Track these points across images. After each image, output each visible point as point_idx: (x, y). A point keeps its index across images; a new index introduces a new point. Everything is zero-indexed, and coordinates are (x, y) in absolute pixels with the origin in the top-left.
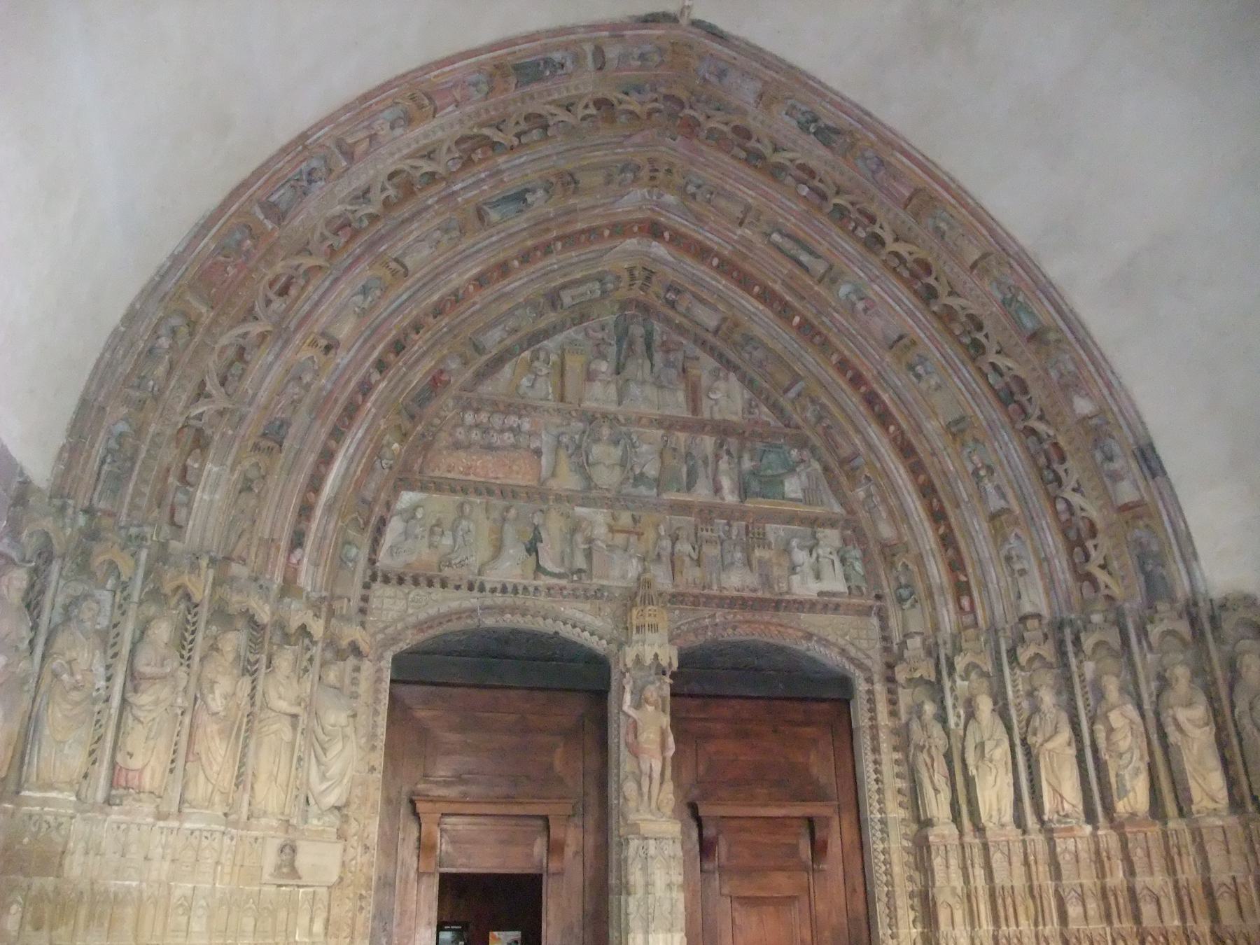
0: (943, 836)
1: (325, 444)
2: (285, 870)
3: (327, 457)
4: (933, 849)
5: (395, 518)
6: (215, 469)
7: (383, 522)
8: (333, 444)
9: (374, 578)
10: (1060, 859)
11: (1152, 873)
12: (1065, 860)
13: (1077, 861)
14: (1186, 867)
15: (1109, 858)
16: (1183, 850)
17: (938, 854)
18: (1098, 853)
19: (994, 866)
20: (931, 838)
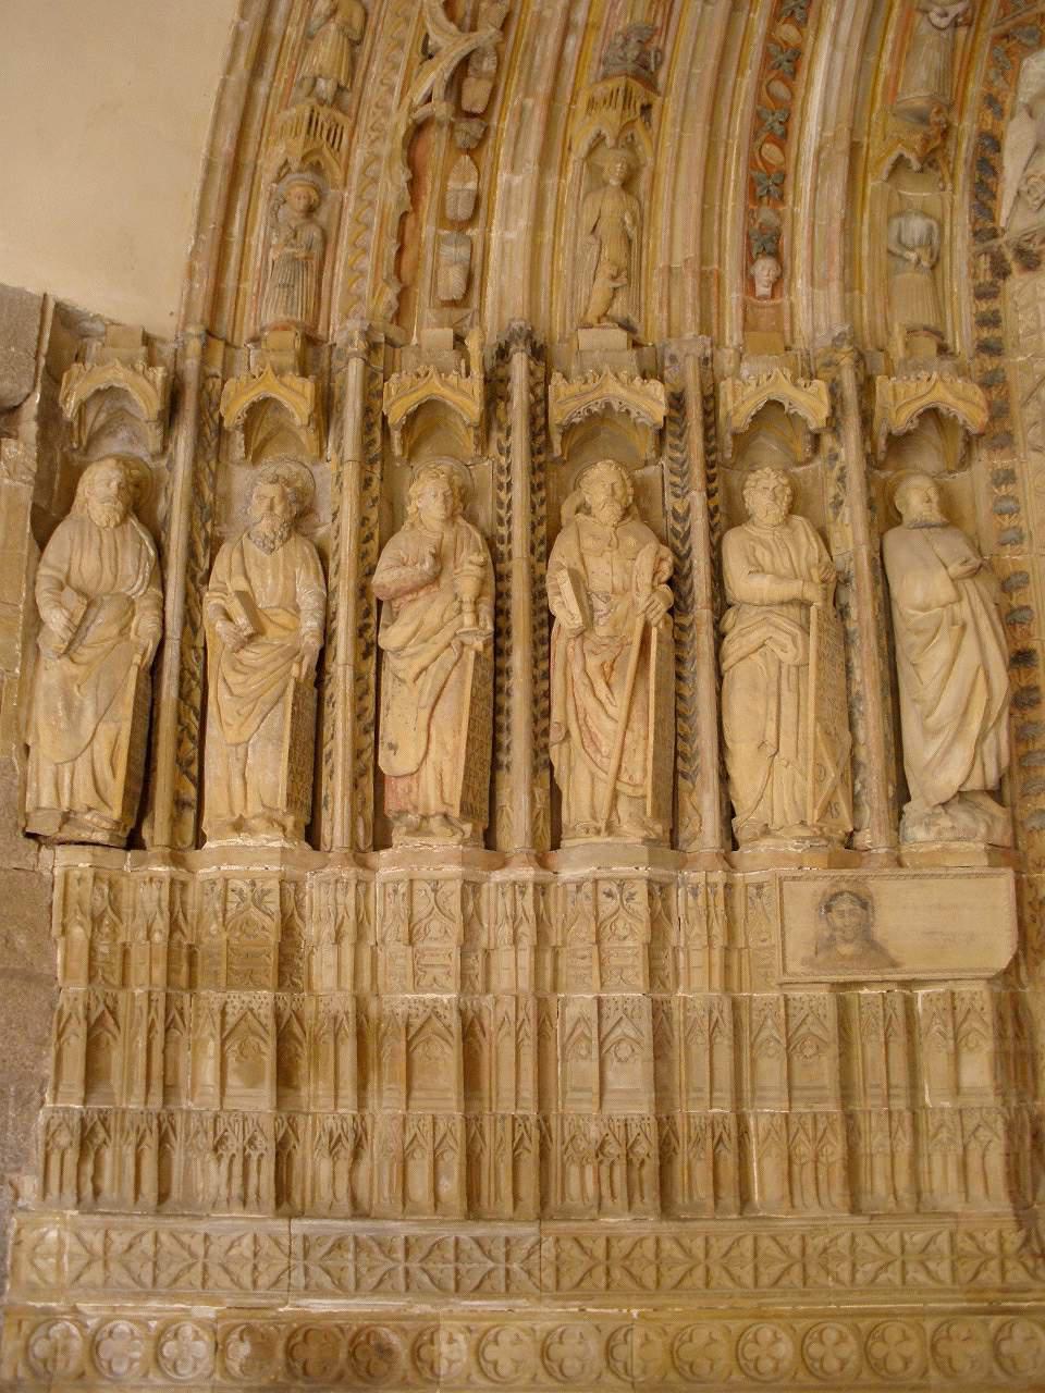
1: (769, 37)
2: (846, 949)
3: (786, 64)
5: (1016, 120)
6: (517, 180)
7: (990, 147)
8: (788, 32)
9: (1000, 271)
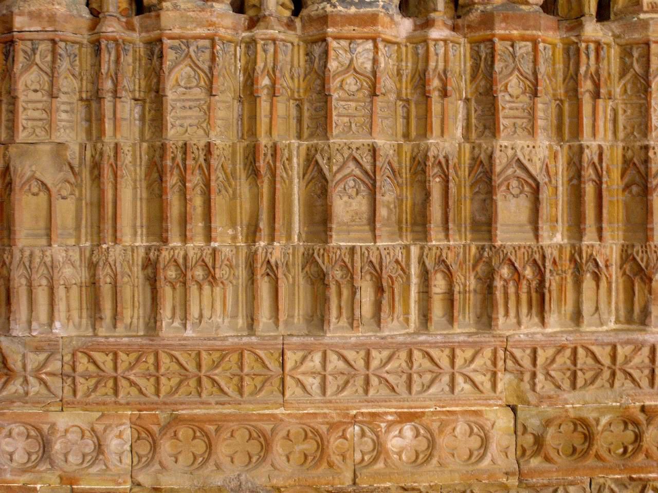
0: (52, 18)
4: (21, 47)
10: (334, 84)
11: (532, 132)
12: (345, 93)
13: (373, 94)
14: (600, 123)
15: (444, 94)
16: (603, 91)
17: (30, 63)
18: (421, 80)
19: (171, 95)
20: (19, 22)
